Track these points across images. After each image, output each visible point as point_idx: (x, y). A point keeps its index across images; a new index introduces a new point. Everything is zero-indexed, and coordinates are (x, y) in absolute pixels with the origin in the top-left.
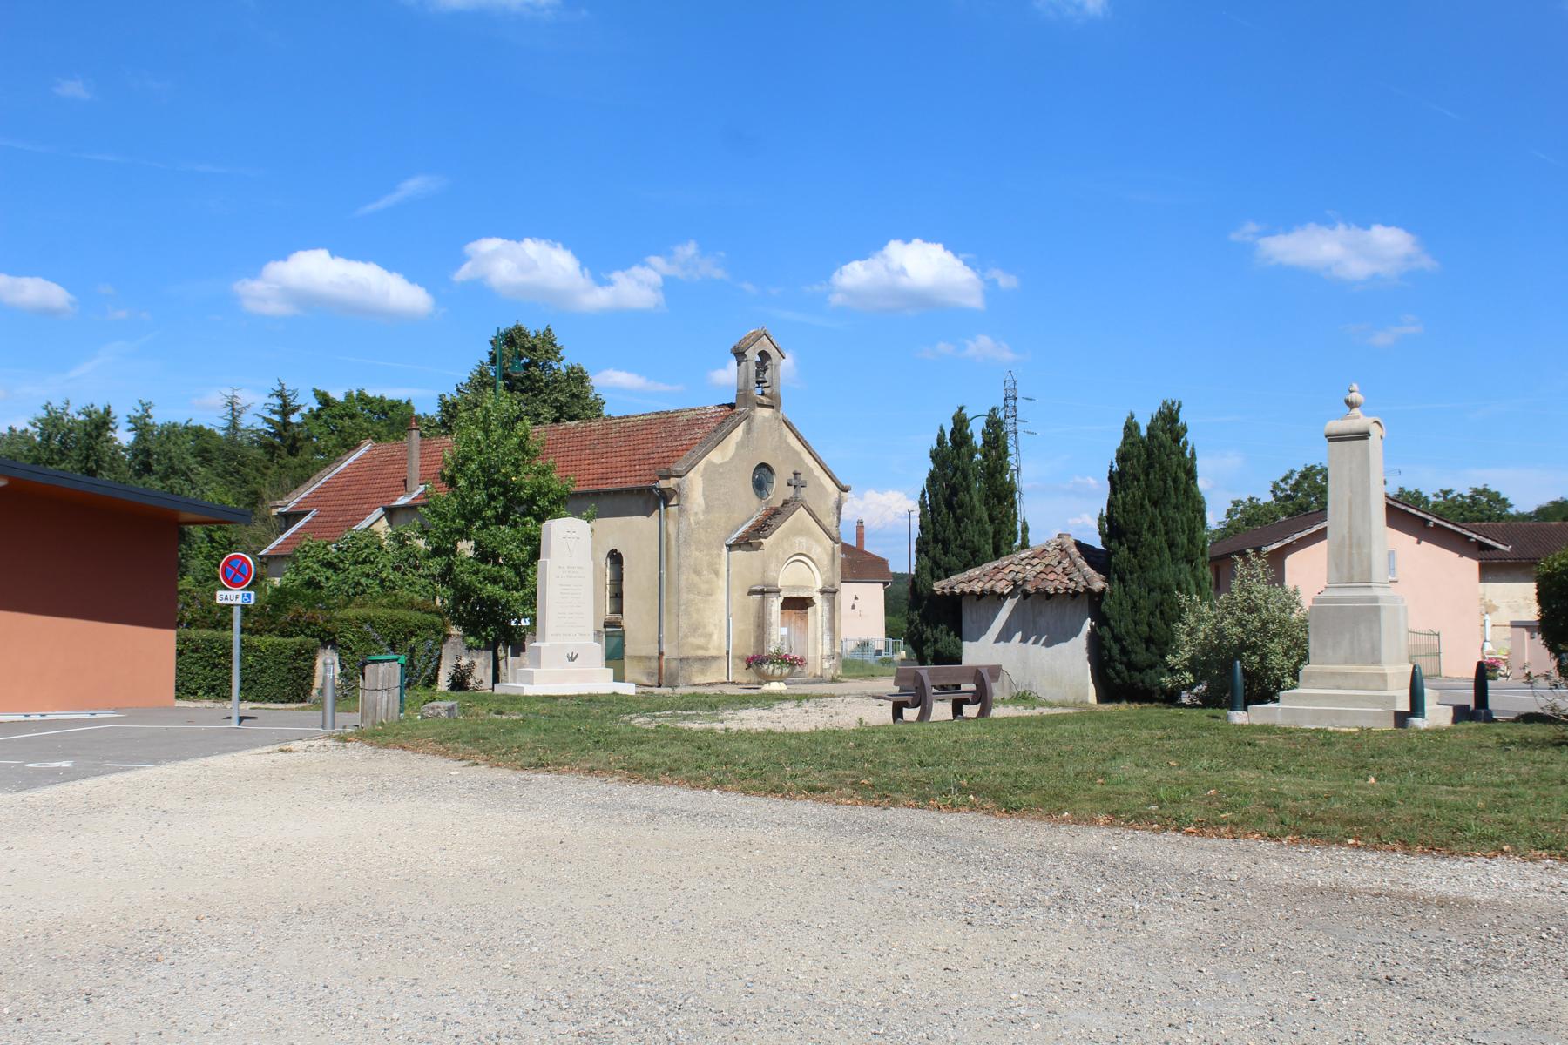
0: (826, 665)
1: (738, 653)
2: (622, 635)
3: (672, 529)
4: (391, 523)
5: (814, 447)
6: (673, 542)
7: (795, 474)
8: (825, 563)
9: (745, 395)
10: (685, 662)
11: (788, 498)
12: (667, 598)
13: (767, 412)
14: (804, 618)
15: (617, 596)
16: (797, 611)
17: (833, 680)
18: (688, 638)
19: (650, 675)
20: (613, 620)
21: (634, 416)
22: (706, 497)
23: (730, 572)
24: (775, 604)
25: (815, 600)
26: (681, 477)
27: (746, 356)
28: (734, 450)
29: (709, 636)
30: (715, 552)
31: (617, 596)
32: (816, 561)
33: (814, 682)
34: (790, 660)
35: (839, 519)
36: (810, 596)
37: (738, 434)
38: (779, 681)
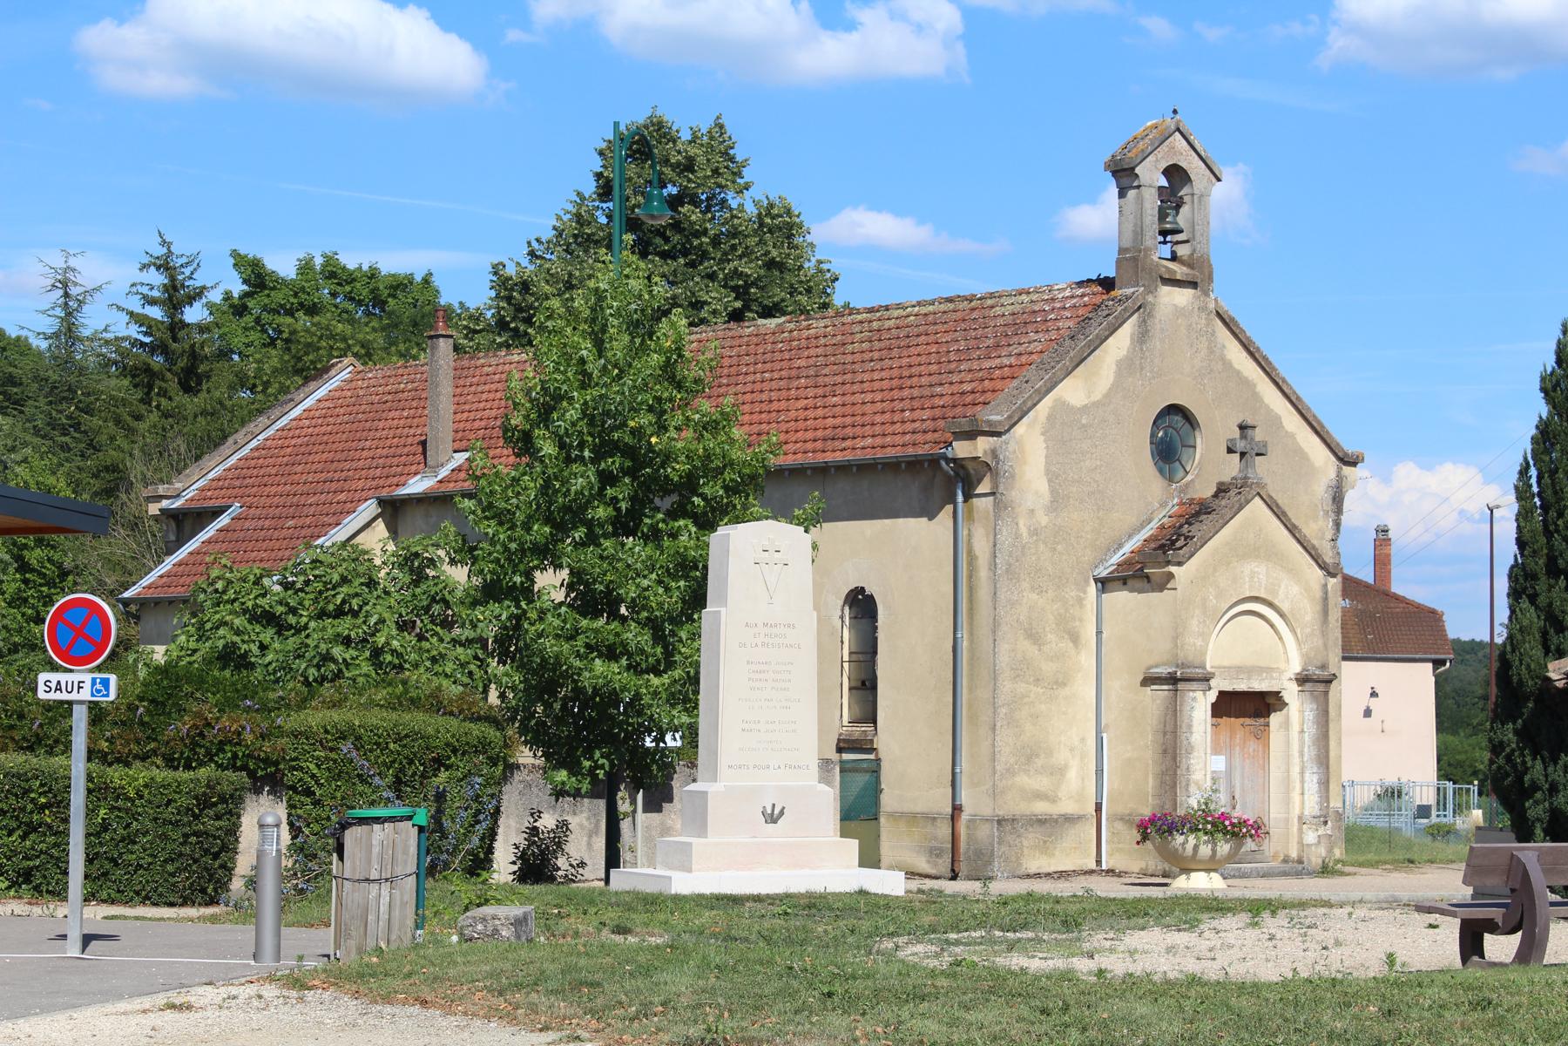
0: (1310, 837)
1: (1121, 809)
2: (875, 769)
3: (981, 546)
4: (394, 532)
5: (1283, 370)
6: (983, 573)
7: (1243, 427)
8: (1308, 618)
9: (1135, 259)
10: (1009, 828)
11: (1226, 479)
12: (971, 690)
13: (1183, 296)
14: (1262, 736)
15: (866, 686)
16: (1248, 721)
17: (1325, 870)
18: (1014, 774)
19: (934, 853)
20: (856, 736)
21: (899, 306)
22: (1052, 477)
23: (1104, 636)
24: (1200, 705)
25: (1286, 697)
26: (999, 434)
27: (1137, 176)
29: (1060, 772)
30: (1070, 593)
31: (866, 686)
33: (1285, 874)
34: (1232, 824)
35: (1337, 524)
36: (1275, 689)
37: (1120, 342)
38: (1208, 871)
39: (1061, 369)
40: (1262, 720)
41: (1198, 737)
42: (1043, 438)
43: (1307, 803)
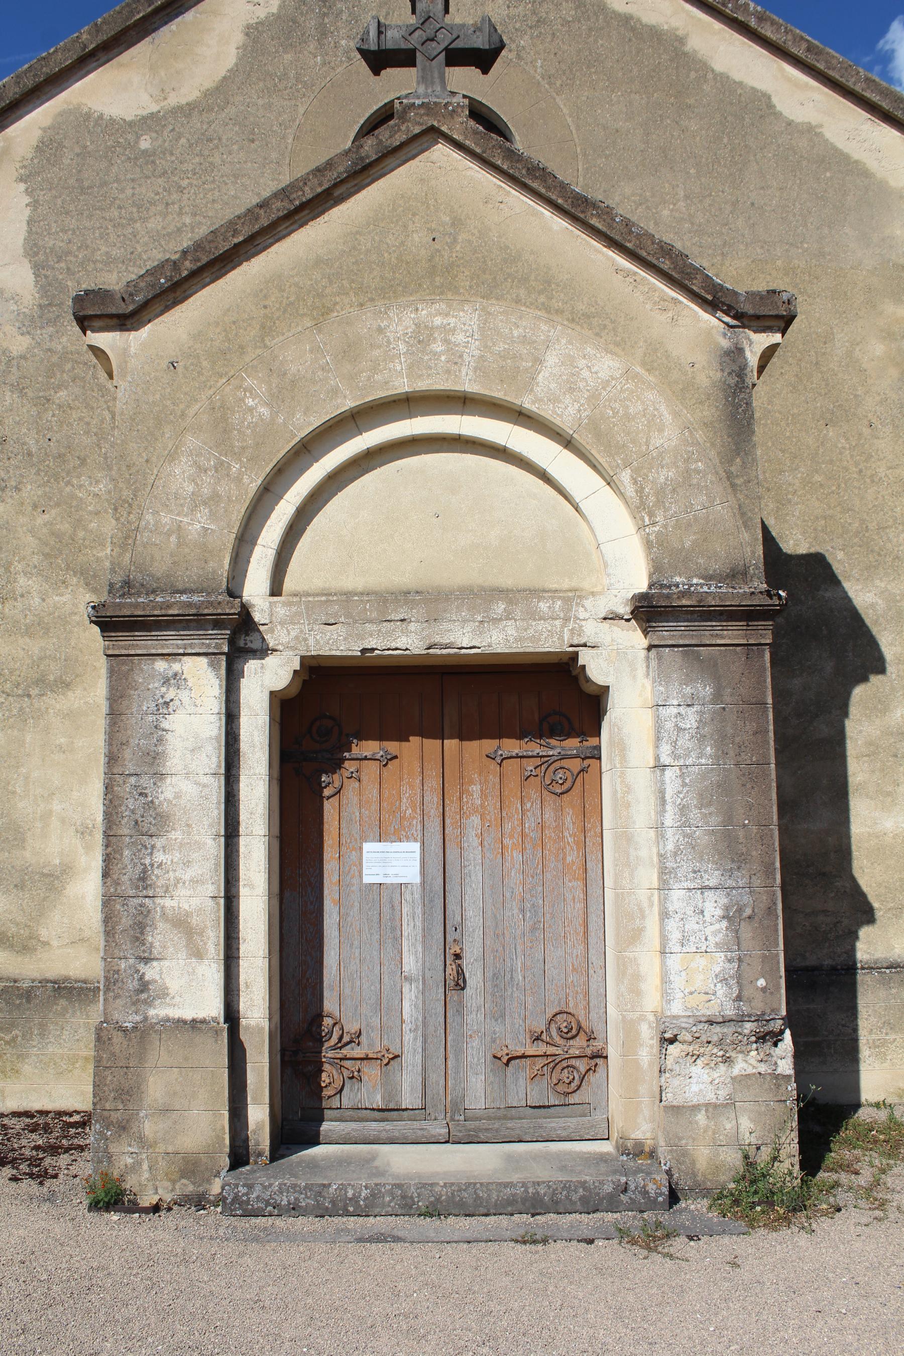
16: (512, 746)
28: (230, 58)
32: (583, 439)
39: (65, 49)
40: (572, 744)
41: (187, 788)
42: (22, 186)
43: (678, 982)
